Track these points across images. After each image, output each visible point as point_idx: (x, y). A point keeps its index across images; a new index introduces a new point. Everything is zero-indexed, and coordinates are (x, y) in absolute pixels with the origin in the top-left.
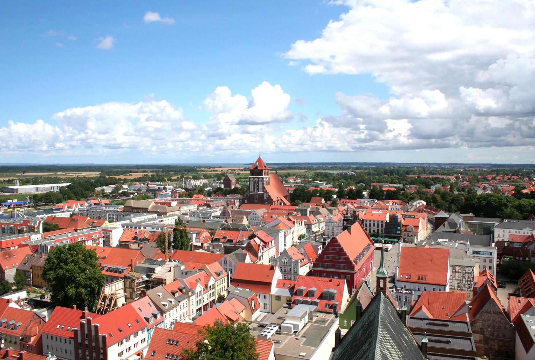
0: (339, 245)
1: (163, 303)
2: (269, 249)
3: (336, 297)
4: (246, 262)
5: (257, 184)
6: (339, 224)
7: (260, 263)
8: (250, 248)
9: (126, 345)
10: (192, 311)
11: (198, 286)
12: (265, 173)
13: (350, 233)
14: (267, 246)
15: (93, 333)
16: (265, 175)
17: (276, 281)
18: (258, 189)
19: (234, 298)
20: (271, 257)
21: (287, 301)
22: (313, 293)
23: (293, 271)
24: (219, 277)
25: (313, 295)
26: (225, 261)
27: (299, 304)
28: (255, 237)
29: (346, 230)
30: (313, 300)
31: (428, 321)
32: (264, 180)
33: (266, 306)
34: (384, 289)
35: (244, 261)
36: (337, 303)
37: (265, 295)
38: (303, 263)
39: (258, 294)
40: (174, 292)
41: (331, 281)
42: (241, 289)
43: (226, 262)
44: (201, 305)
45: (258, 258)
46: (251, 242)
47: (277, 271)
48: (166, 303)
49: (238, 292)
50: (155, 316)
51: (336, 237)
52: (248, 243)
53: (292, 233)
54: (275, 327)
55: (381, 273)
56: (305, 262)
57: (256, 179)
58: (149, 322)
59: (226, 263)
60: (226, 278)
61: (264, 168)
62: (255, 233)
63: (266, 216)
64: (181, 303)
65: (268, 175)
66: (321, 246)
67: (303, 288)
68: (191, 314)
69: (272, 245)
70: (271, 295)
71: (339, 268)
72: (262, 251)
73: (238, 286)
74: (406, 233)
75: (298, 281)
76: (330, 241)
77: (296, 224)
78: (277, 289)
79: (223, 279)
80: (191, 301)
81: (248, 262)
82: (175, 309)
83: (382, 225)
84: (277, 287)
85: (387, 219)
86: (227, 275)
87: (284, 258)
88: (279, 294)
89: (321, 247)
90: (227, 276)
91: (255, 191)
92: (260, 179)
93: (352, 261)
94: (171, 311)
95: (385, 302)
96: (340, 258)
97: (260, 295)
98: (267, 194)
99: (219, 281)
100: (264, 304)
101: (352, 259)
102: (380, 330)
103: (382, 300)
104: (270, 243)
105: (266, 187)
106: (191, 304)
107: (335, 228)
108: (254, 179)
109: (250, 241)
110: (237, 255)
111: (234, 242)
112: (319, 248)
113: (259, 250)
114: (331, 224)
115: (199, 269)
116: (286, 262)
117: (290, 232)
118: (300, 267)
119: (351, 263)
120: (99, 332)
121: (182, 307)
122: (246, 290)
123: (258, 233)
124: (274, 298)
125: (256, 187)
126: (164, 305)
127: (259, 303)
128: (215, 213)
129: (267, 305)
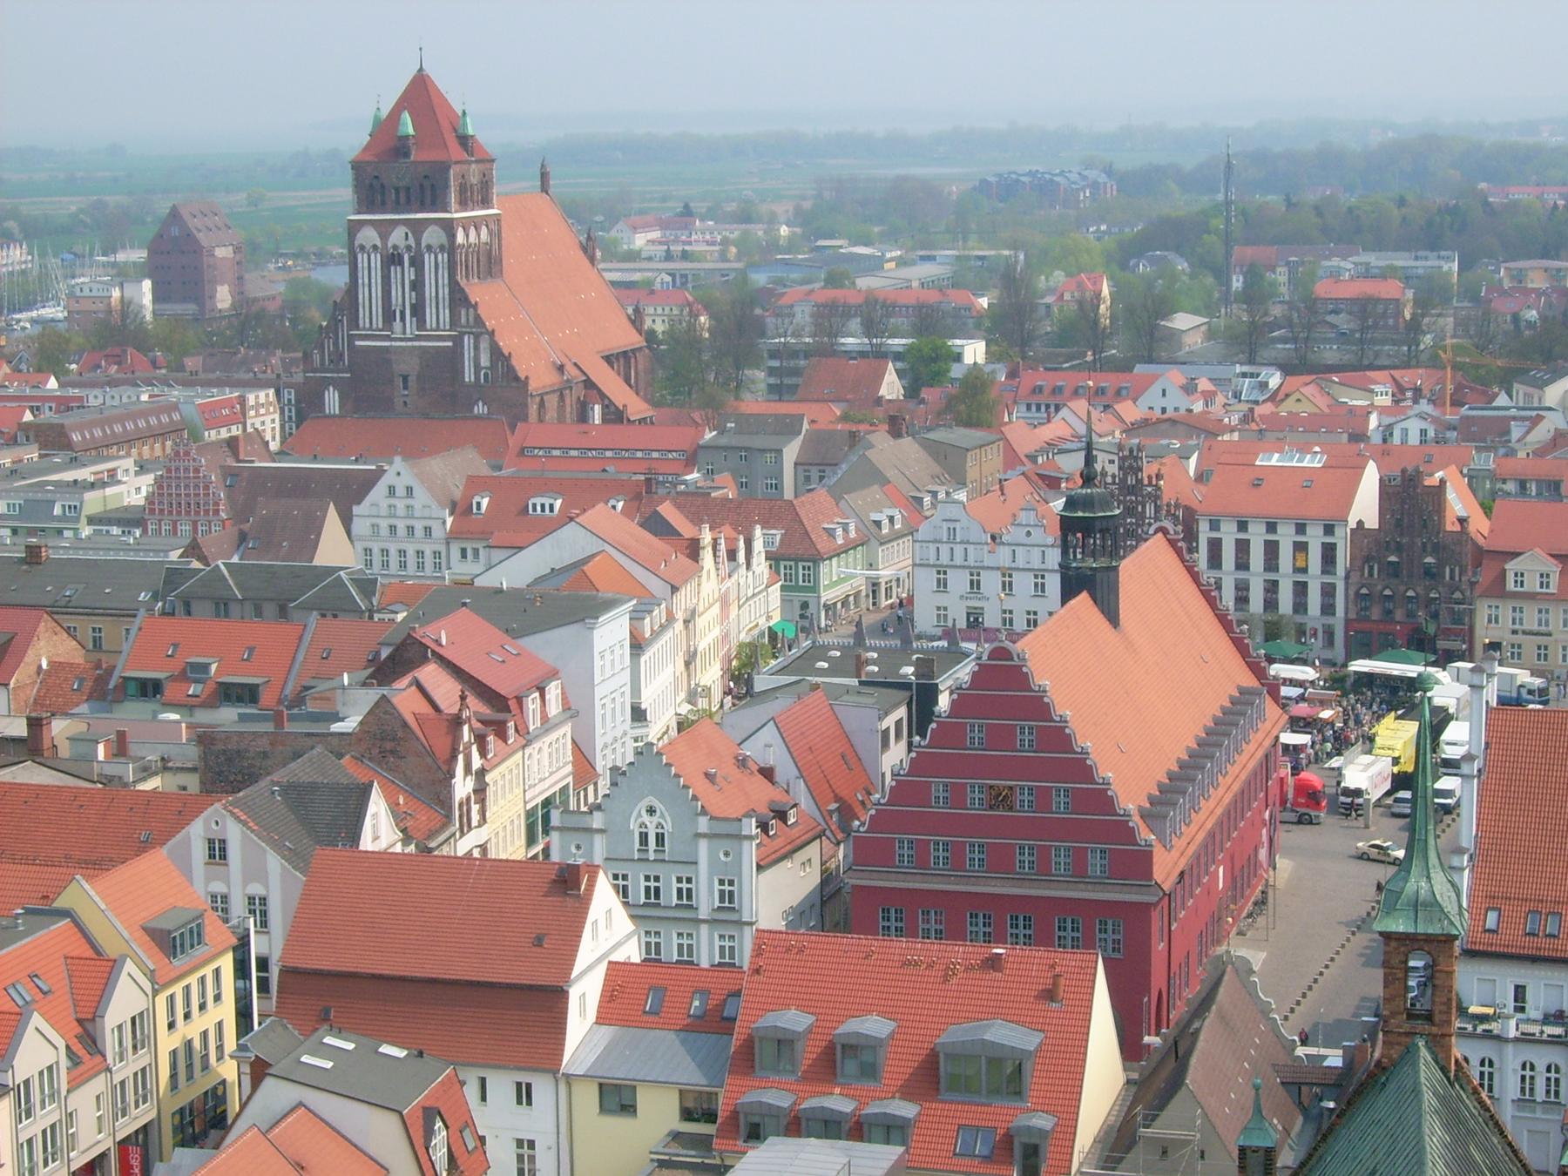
0: (1038, 707)
2: (528, 743)
3: (1033, 1079)
4: (367, 843)
5: (410, 274)
6: (1019, 550)
7: (464, 845)
8: (389, 745)
11: (30, 1032)
12: (463, 189)
13: (1113, 618)
14: (511, 724)
16: (464, 204)
17: (601, 970)
18: (418, 310)
20: (539, 800)
21: (687, 1115)
22: (867, 1057)
23: (706, 902)
24: (180, 962)
25: (870, 1071)
26: (211, 842)
27: (771, 1139)
28: (424, 660)
29: (1084, 595)
30: (874, 1108)
32: (460, 238)
33: (532, 1159)
34: (1437, 1018)
35: (354, 836)
36: (1043, 1122)
37: (524, 1078)
38: (778, 843)
39: (471, 1078)
41: (994, 963)
42: (350, 1046)
43: (223, 850)
45: (448, 818)
46: (395, 700)
47: (604, 897)
49: (329, 1065)
51: (1017, 648)
52: (377, 704)
53: (679, 626)
55: (1416, 905)
56: (795, 832)
57: (398, 237)
59: (224, 857)
60: (227, 963)
61: (456, 152)
62: (425, 633)
63: (485, 502)
65: (486, 202)
66: (901, 712)
67: (795, 1020)
69: (545, 718)
70: (567, 1076)
71: (1043, 867)
72: (477, 762)
73: (324, 1018)
74: (1506, 611)
75: (757, 971)
76: (975, 675)
77: (707, 556)
78: (607, 1032)
79: (208, 971)
81: (381, 845)
83: (1329, 553)
84: (601, 1019)
85: (1366, 506)
86: (234, 941)
87: (642, 806)
88: (619, 1072)
89: (898, 723)
90: (235, 949)
91: (397, 325)
92: (433, 236)
93: (1136, 821)
95: (1452, 1118)
96: (1042, 799)
97: (483, 1081)
98: (484, 344)
99: (177, 989)
100: (520, 1143)
101: (1130, 798)
103: (1428, 1099)
104: (532, 703)
105: (476, 291)
107: (992, 582)
108: (384, 237)
109: (385, 691)
110: (297, 795)
111: (266, 698)
112: (886, 732)
113: (454, 758)
114: (959, 550)
115: (29, 912)
116: (660, 839)
117: (671, 618)
118: (760, 868)
119: (1129, 834)
122: (386, 1049)
123: (442, 634)
124: (587, 1097)
125: (401, 296)
127: (482, 1139)
128: (109, 491)
129: (539, 1151)
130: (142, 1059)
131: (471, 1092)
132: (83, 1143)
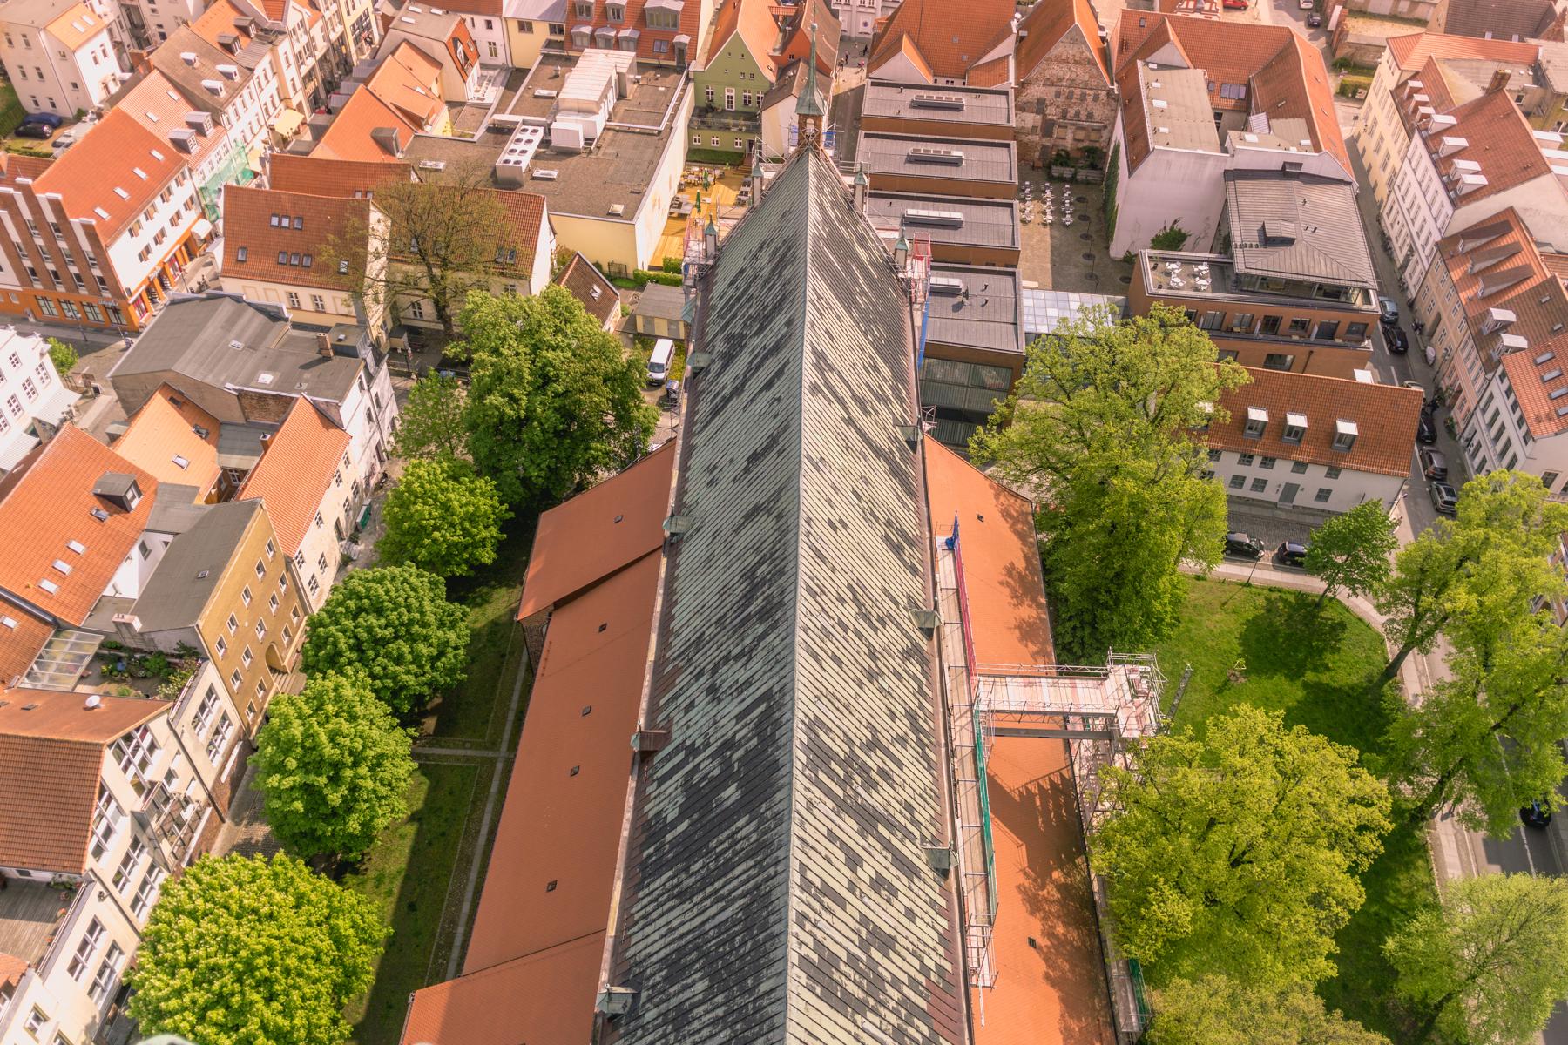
1: (207, 83)
9: (148, 230)
10: (294, 86)
15: (51, 218)
19: (404, 44)
31: (913, 95)
36: (685, 39)
37: (489, 18)
40: (228, 41)
44: (311, 62)
48: (217, 84)
50: (199, 129)
54: (535, 131)
58: (188, 152)
64: (258, 72)
68: (291, 92)
80: (282, 58)
82: (245, 92)
88: (524, 16)
94: (238, 101)
102: (811, 283)
106: (284, 65)
120: (68, 214)
121: (263, 82)
122: (435, 11)
124: (514, 26)
126: (214, 92)
129: (498, 47)
130: (334, 7)
131: (468, 24)
132: (319, 48)
